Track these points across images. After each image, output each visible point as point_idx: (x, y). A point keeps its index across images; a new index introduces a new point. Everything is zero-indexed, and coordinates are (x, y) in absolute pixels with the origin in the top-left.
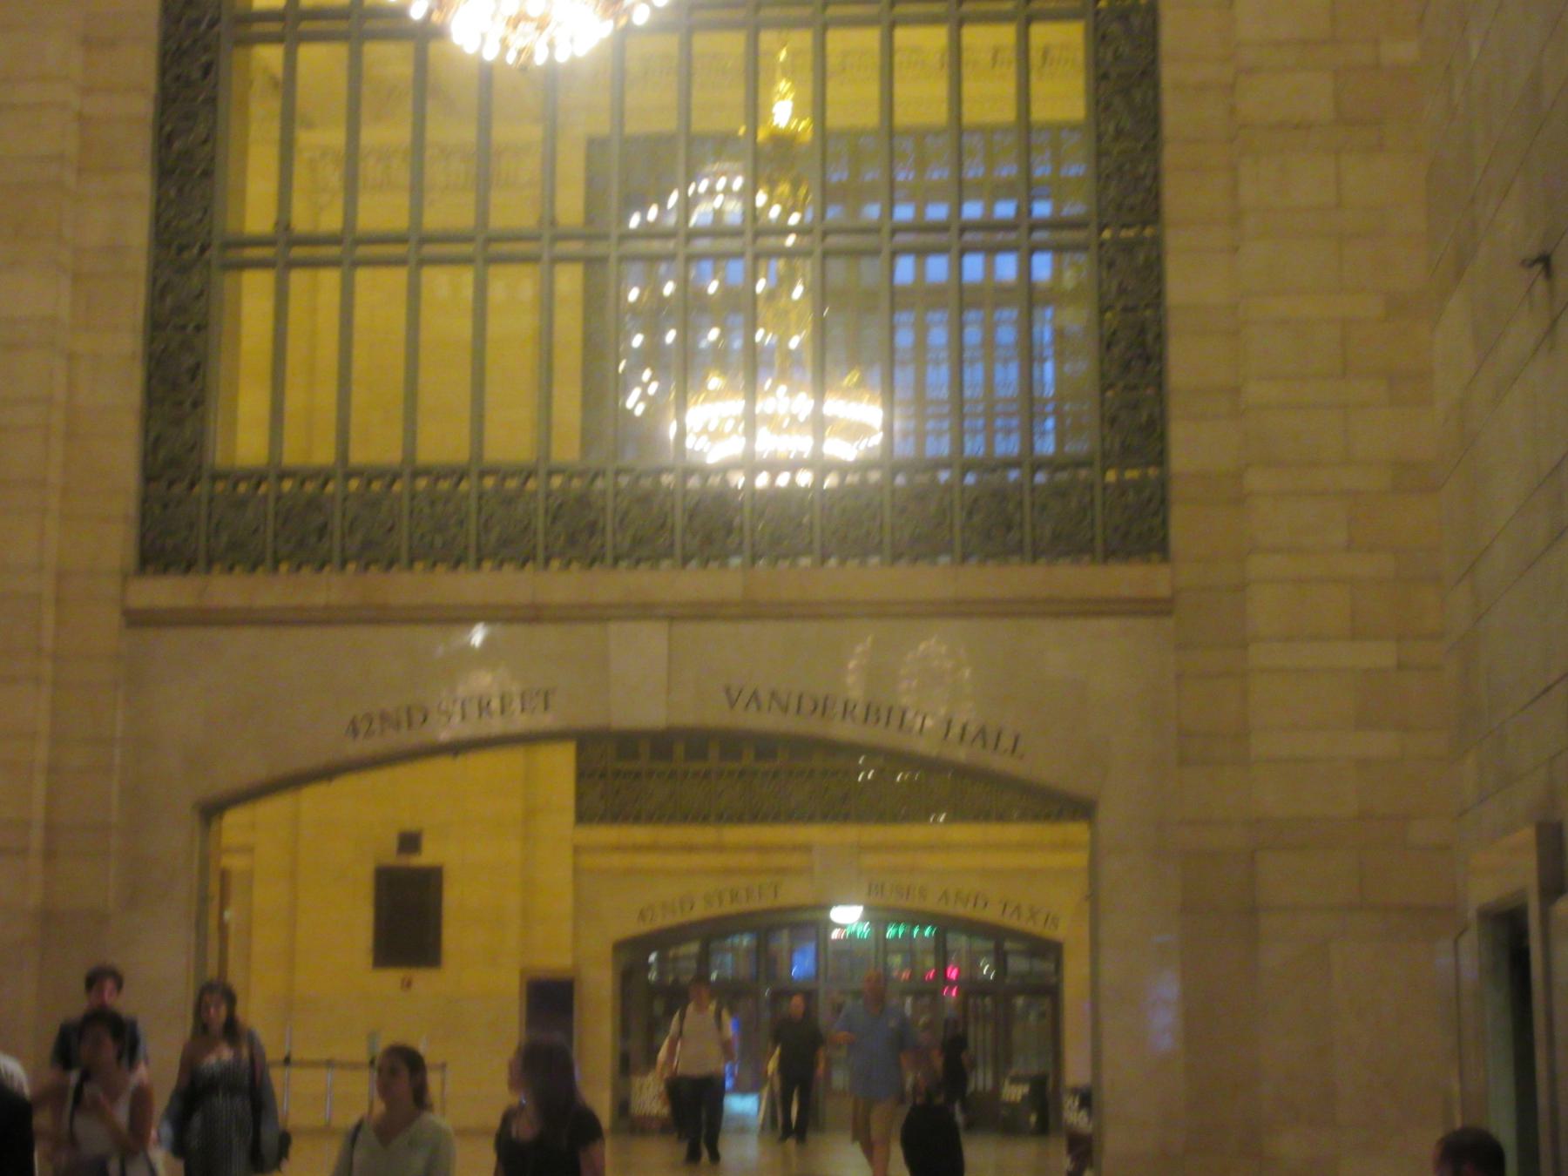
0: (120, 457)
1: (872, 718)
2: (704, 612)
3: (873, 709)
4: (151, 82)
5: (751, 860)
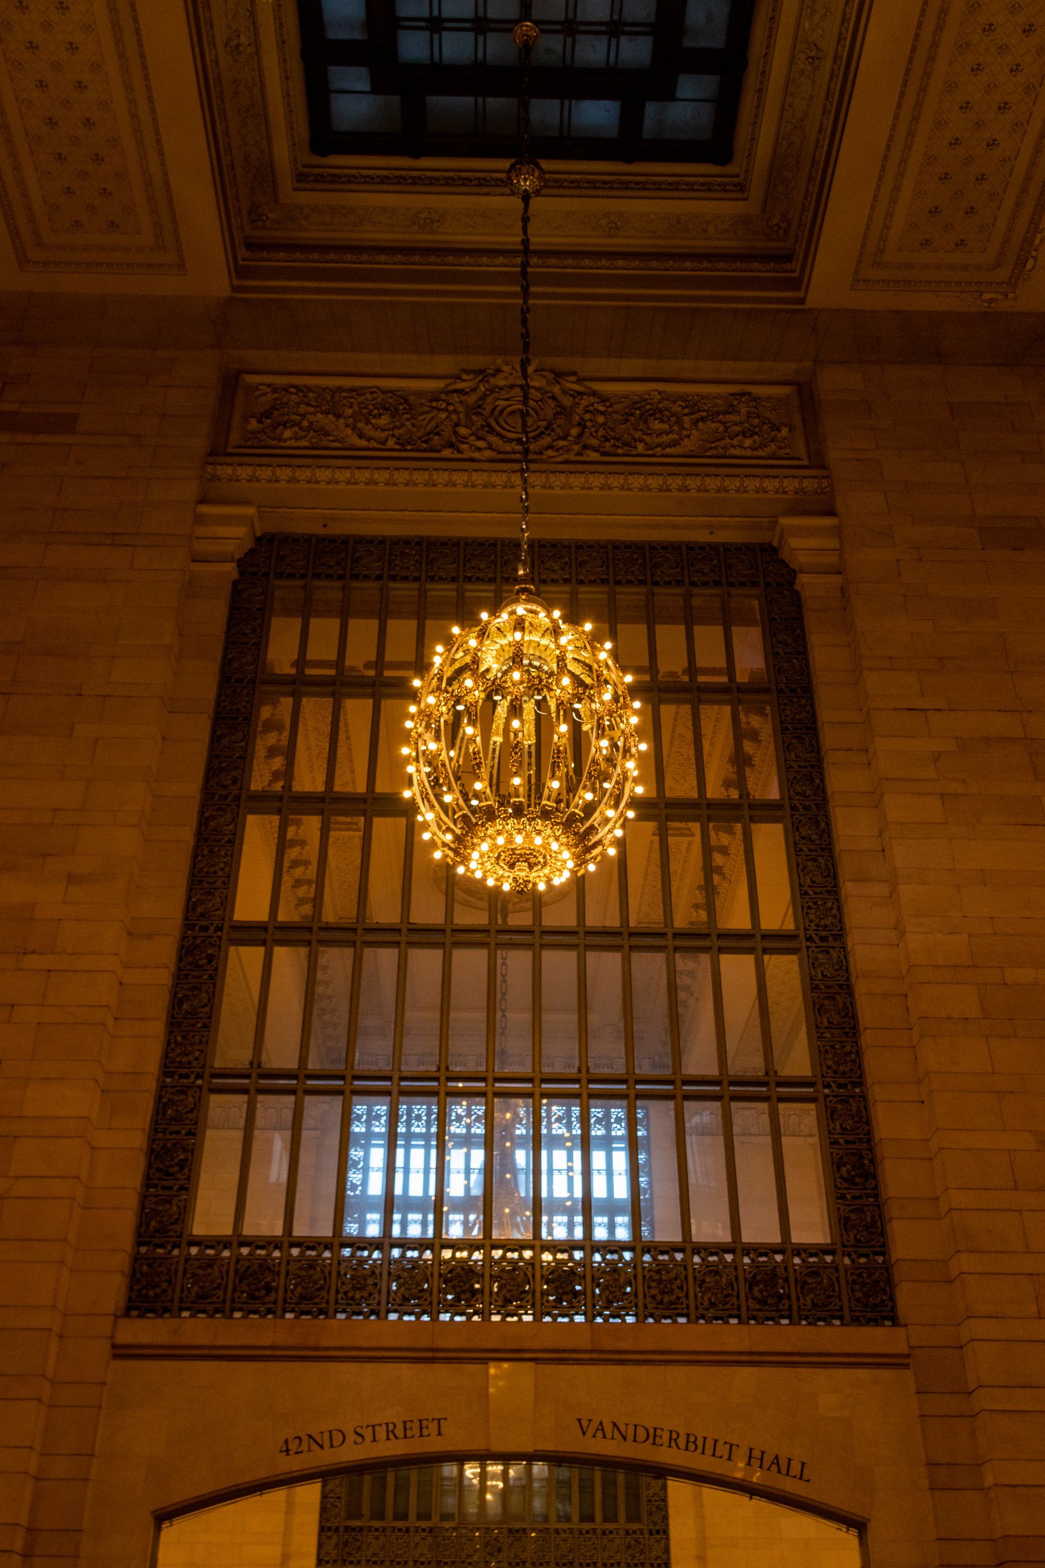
0: (122, 1224)
1: (692, 1447)
3: (692, 1439)
4: (172, 962)
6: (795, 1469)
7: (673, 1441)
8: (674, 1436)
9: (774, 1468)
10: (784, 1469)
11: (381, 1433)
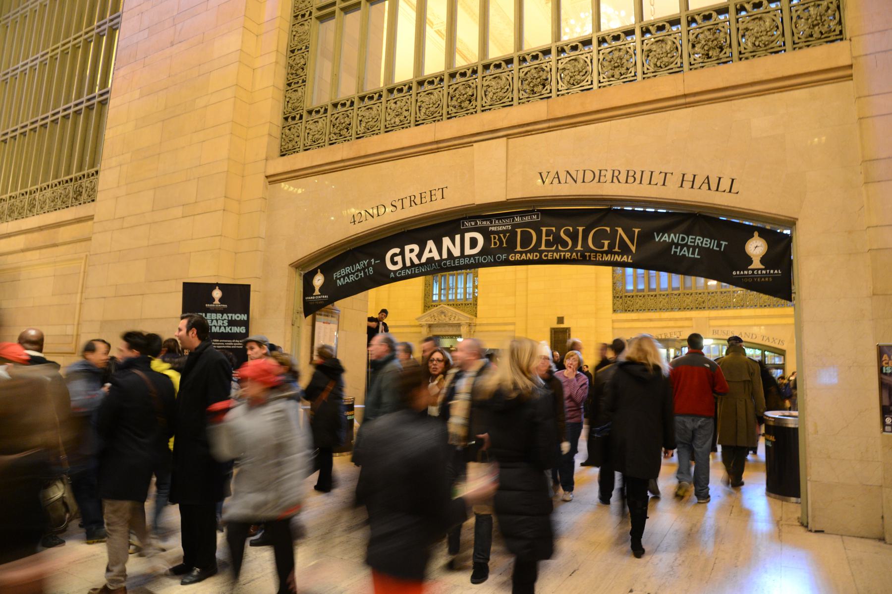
1: (631, 179)
2: (526, 129)
3: (631, 173)
5: (671, 324)
6: (725, 184)
7: (615, 178)
8: (616, 173)
9: (705, 186)
10: (714, 186)
11: (407, 202)
